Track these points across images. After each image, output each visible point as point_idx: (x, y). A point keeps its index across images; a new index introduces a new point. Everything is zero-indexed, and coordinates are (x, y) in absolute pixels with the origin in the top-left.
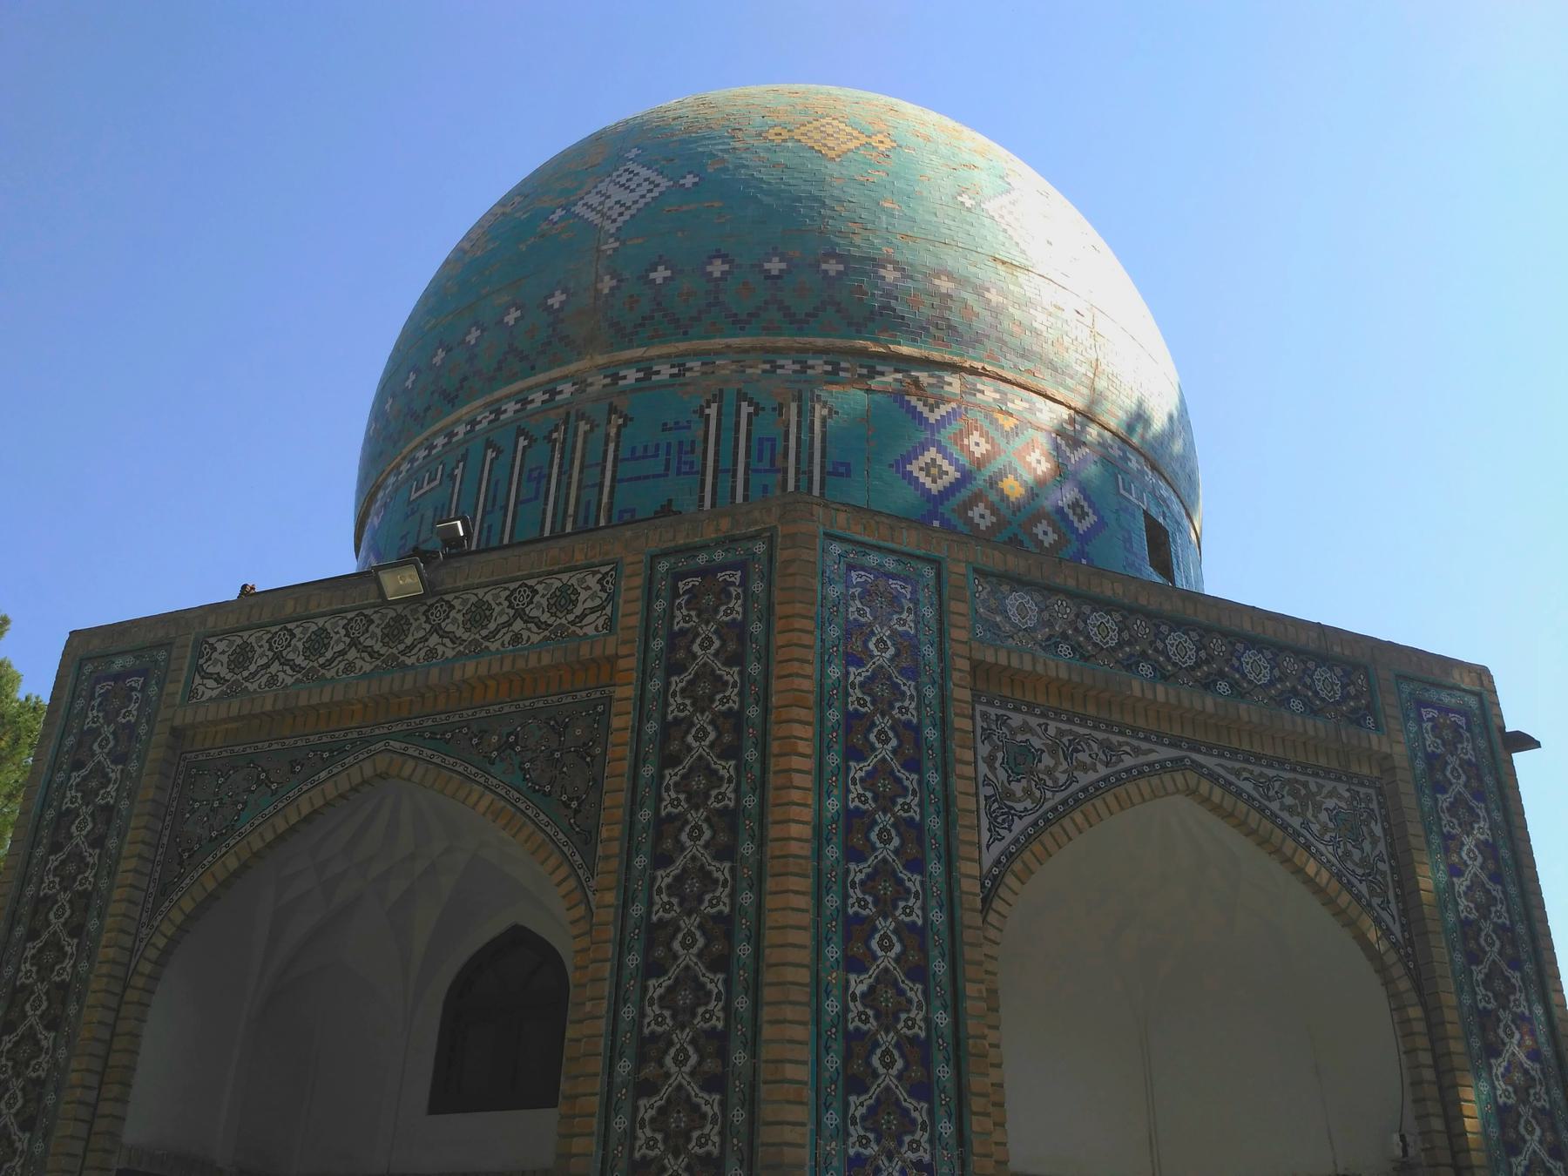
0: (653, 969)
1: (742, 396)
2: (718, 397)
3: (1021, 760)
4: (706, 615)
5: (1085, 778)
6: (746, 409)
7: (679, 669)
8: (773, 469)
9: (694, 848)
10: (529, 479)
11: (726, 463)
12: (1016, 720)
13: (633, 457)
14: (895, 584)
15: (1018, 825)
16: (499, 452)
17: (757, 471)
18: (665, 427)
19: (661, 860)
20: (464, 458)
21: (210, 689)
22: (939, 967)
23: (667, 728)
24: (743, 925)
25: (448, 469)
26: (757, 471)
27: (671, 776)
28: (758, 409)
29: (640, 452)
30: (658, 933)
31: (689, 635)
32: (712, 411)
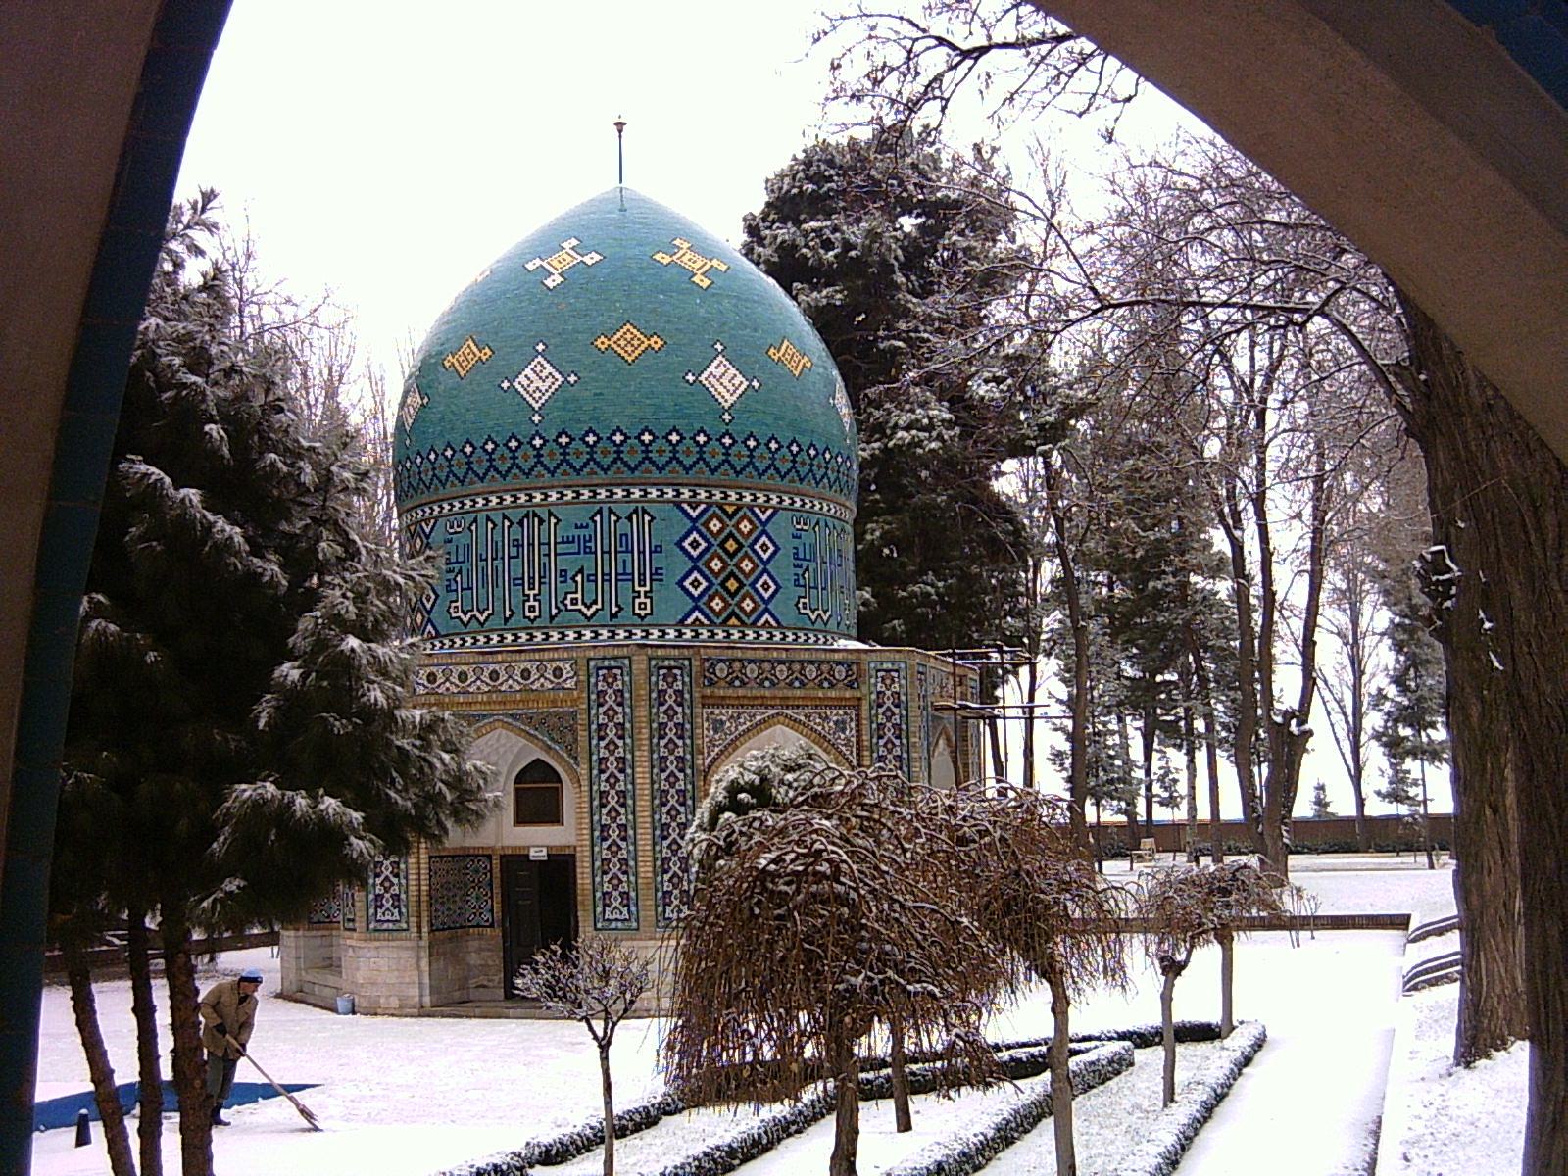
0: (602, 805)
1: (611, 511)
2: (600, 511)
3: (718, 726)
4: (610, 686)
5: (741, 728)
6: (613, 518)
7: (600, 705)
8: (627, 551)
9: (612, 768)
11: (606, 549)
12: (717, 711)
13: (563, 542)
14: (676, 671)
15: (717, 749)
16: (495, 525)
18: (577, 527)
19: (601, 772)
21: (421, 690)
22: (690, 802)
23: (599, 726)
24: (629, 795)
27: (602, 744)
28: (619, 518)
30: (603, 794)
31: (605, 692)
32: (598, 518)
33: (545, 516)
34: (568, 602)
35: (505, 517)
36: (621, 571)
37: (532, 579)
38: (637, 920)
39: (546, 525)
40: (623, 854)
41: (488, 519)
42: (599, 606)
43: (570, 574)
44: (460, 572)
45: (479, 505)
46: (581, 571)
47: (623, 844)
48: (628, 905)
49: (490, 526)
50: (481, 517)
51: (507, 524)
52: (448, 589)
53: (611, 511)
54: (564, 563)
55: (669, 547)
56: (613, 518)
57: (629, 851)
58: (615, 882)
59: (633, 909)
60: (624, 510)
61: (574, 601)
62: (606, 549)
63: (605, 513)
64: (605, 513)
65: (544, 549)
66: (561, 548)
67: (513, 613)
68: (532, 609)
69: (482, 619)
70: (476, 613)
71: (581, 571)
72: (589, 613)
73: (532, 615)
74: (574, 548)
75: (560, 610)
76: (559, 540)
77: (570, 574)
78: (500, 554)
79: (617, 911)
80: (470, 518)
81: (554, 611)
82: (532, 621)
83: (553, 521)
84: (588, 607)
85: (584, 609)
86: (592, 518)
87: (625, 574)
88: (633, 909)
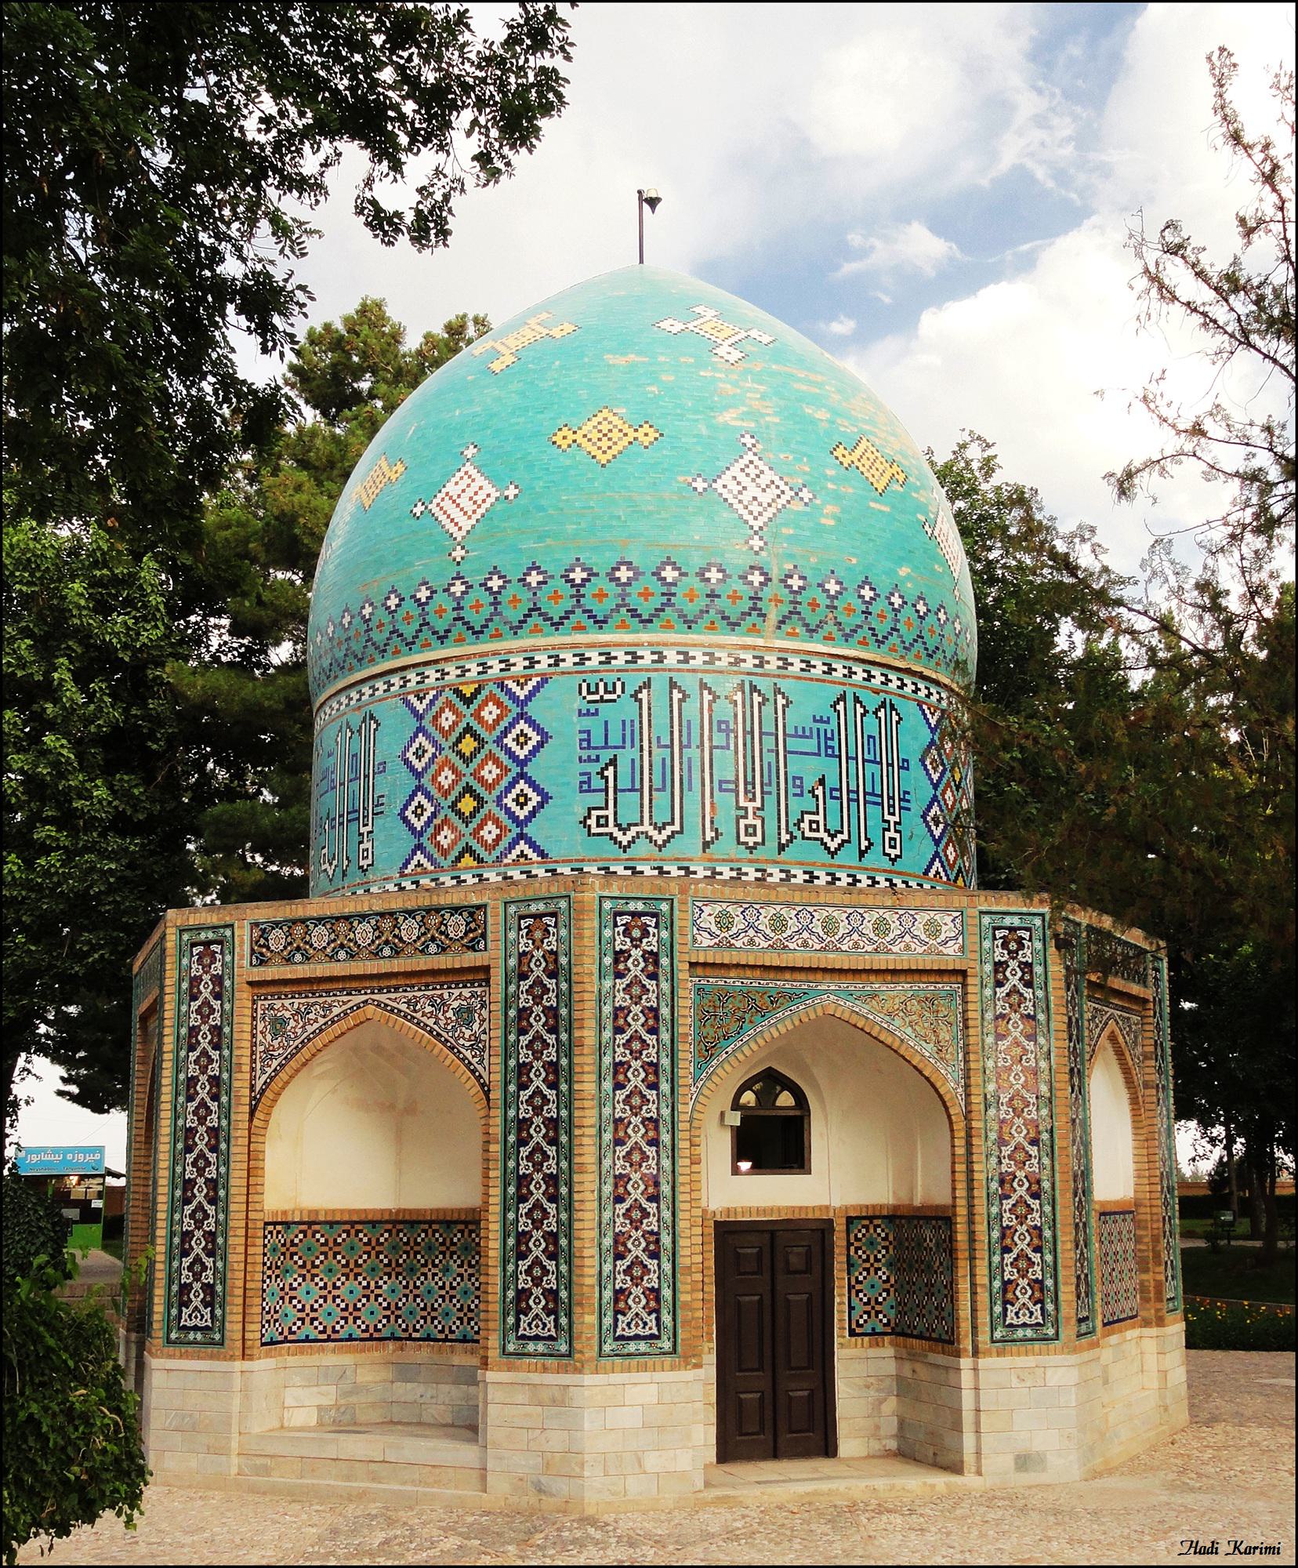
1: (857, 700)
2: (843, 698)
10: (720, 730)
13: (796, 736)
17: (869, 761)
20: (647, 685)
25: (630, 690)
26: (869, 761)
29: (800, 733)
33: (770, 695)
34: (805, 825)
35: (703, 686)
36: (869, 789)
37: (750, 784)
38: (1056, 1324)
39: (768, 709)
40: (1035, 1219)
41: (673, 685)
42: (845, 837)
43: (807, 787)
44: (613, 762)
45: (722, 664)
46: (822, 782)
47: (1035, 1204)
48: (1041, 1301)
49: (677, 695)
50: (660, 682)
51: (707, 697)
52: (586, 787)
53: (857, 700)
54: (796, 766)
55: (914, 763)
56: (860, 710)
57: (1042, 1214)
58: (1022, 1264)
59: (1050, 1307)
60: (872, 701)
61: (814, 826)
62: (852, 754)
63: (850, 698)
64: (850, 698)
65: (769, 742)
66: (794, 744)
67: (718, 834)
68: (751, 830)
69: (660, 838)
70: (647, 827)
71: (822, 782)
72: (833, 845)
73: (751, 841)
74: (811, 745)
75: (793, 838)
76: (790, 731)
77: (807, 787)
78: (695, 741)
79: (1024, 1311)
80: (634, 681)
81: (785, 837)
82: (751, 849)
83: (781, 701)
84: (833, 837)
85: (827, 839)
86: (834, 706)
87: (873, 794)
88: (1050, 1307)
